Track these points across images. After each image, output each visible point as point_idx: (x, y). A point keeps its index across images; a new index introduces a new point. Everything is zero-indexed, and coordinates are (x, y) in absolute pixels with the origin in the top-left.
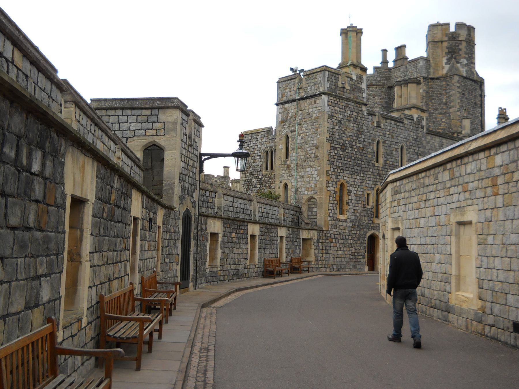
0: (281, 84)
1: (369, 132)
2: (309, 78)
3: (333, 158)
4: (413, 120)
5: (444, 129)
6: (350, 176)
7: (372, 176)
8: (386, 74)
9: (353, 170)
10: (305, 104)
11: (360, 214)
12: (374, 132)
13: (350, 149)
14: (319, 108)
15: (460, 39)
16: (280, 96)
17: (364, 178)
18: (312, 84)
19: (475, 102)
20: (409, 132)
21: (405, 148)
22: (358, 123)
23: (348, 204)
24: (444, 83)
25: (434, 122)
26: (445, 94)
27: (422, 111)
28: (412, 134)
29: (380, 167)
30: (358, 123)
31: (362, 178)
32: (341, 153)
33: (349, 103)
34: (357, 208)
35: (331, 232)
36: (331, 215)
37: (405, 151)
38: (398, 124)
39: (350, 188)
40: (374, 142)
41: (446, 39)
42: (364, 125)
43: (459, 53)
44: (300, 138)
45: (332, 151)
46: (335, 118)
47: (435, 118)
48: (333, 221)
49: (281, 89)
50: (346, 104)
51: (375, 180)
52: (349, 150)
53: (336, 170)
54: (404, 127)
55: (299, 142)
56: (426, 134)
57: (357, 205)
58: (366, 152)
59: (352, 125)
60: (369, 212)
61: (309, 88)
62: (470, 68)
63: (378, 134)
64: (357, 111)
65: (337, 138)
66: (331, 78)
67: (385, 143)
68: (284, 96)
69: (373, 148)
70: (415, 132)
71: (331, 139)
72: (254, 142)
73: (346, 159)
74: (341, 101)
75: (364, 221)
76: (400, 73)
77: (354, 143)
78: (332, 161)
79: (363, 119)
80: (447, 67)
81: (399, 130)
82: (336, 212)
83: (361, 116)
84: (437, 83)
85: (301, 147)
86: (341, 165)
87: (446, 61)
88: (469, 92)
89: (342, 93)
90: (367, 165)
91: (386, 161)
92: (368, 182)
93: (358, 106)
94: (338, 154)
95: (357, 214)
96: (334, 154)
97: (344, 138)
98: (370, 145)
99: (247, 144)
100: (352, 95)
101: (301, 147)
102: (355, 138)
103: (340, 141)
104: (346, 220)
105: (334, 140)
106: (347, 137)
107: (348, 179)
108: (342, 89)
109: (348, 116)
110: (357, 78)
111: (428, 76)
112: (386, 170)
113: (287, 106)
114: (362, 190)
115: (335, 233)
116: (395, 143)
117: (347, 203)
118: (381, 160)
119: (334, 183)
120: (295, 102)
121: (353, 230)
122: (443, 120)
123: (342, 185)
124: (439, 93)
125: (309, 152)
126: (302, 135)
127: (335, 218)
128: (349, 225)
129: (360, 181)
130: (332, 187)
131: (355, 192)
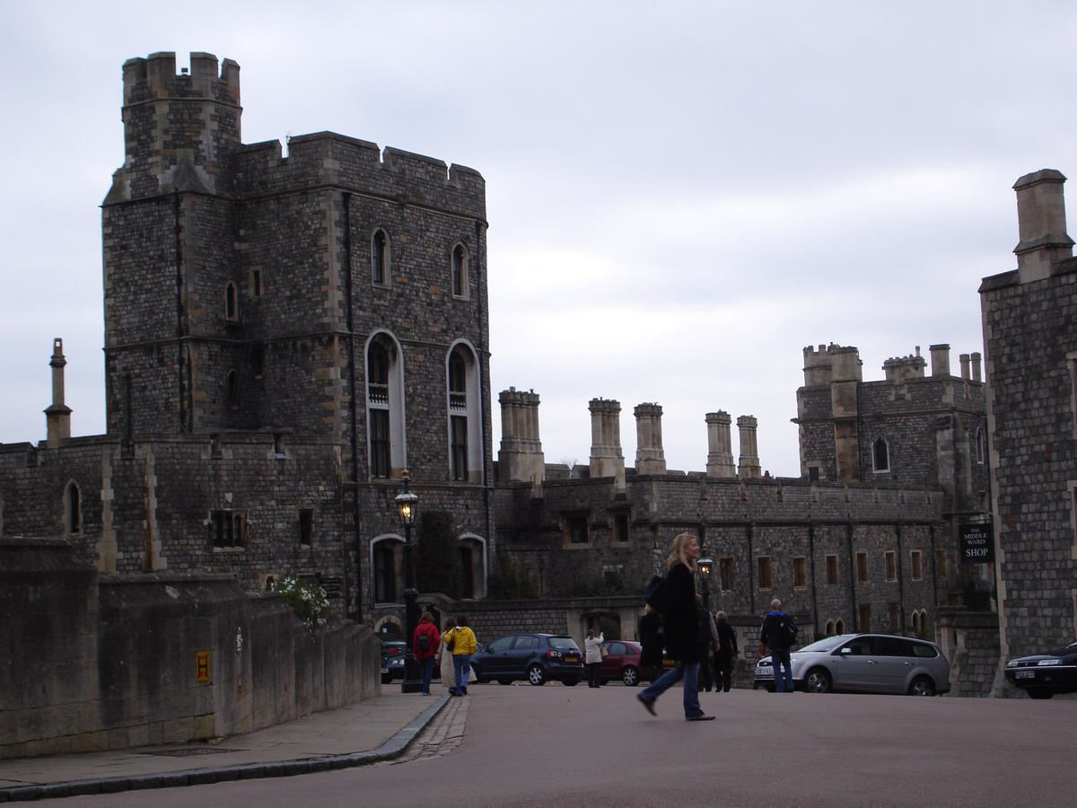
62: (145, 170)
88: (141, 236)
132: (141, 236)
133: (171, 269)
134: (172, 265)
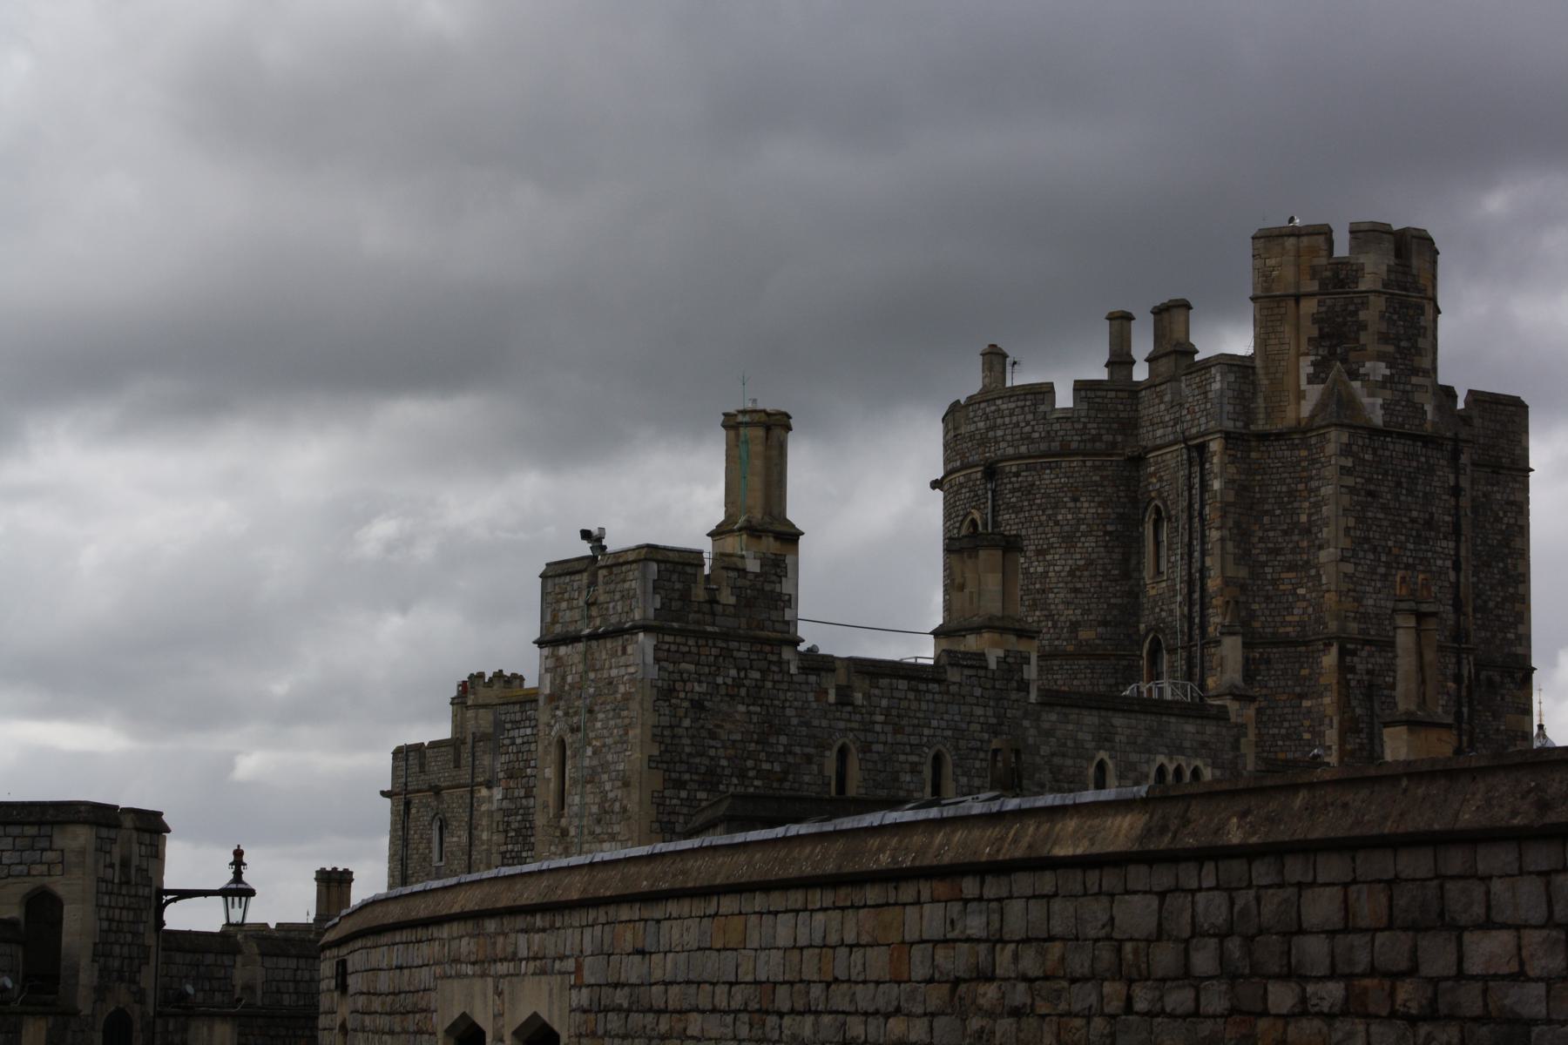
0: (550, 583)
1: (807, 724)
2: (613, 577)
4: (986, 668)
5: (1301, 624)
8: (1121, 407)
10: (603, 650)
12: (825, 723)
13: (735, 781)
14: (632, 670)
15: (1362, 287)
16: (548, 619)
18: (618, 596)
19: (1427, 516)
20: (965, 709)
21: (949, 759)
22: (767, 702)
24: (1304, 453)
25: (1268, 598)
26: (1305, 494)
28: (979, 711)
30: (767, 702)
32: (701, 795)
33: (733, 645)
37: (948, 770)
38: (922, 687)
40: (827, 753)
41: (1314, 286)
42: (788, 704)
43: (1357, 340)
44: (589, 751)
46: (682, 695)
47: (1274, 582)
49: (550, 599)
50: (722, 649)
54: (947, 692)
55: (587, 762)
59: (742, 708)
61: (611, 605)
62: (1404, 392)
63: (842, 725)
64: (764, 665)
65: (689, 755)
66: (669, 580)
67: (870, 751)
68: (558, 622)
69: (821, 772)
70: (991, 703)
71: (667, 757)
72: (529, 731)
74: (701, 642)
76: (1162, 407)
78: (669, 822)
79: (785, 686)
80: (1314, 393)
81: (924, 706)
83: (777, 677)
84: (1279, 454)
85: (591, 778)
87: (1311, 370)
88: (1399, 484)
89: (708, 618)
93: (767, 648)
96: (675, 801)
97: (712, 752)
99: (512, 734)
100: (743, 621)
101: (591, 778)
102: (752, 747)
103: (697, 760)
105: (677, 759)
106: (724, 747)
108: (706, 608)
109: (729, 681)
110: (762, 566)
111: (1246, 425)
113: (563, 650)
116: (908, 749)
120: (581, 644)
122: (1301, 591)
124: (1284, 489)
125: (611, 795)
126: (594, 743)
132: (1399, 484)
133: (1444, 544)
134: (1445, 538)
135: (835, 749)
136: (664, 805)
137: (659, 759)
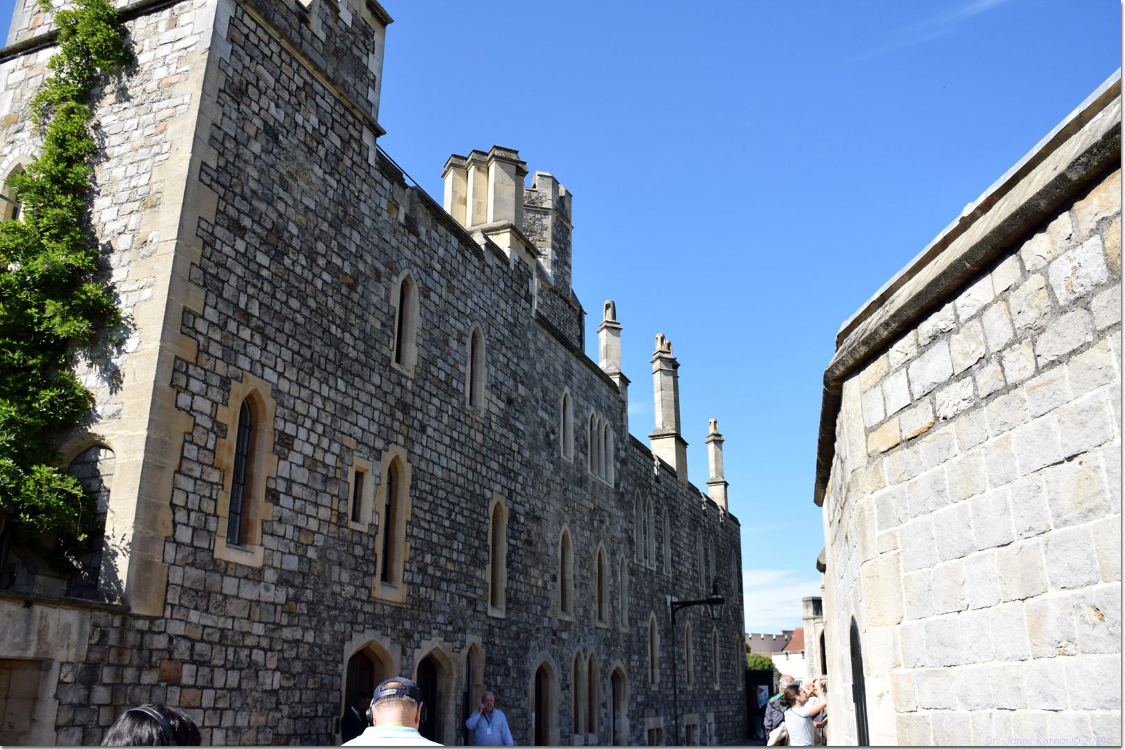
3: (224, 266)
6: (291, 374)
7: (378, 404)
9: (307, 353)
11: (322, 551)
17: (348, 402)
21: (483, 342)
22: (344, 181)
23: (272, 495)
27: (528, 250)
29: (407, 378)
30: (344, 181)
31: (339, 398)
32: (263, 259)
34: (313, 524)
35: (177, 628)
36: (184, 535)
39: (290, 429)
40: (394, 279)
45: (220, 232)
48: (194, 573)
50: (305, 83)
51: (388, 420)
52: (296, 262)
53: (232, 326)
54: (483, 272)
56: (536, 324)
57: (310, 510)
58: (364, 303)
59: (320, 172)
60: (358, 551)
63: (408, 253)
65: (254, 192)
69: (387, 298)
73: (281, 296)
75: (337, 589)
77: (321, 247)
82: (212, 525)
83: (357, 159)
86: (255, 309)
90: (365, 353)
91: (427, 363)
92: (363, 422)
93: (351, 119)
94: (245, 258)
95: (311, 553)
96: (227, 250)
97: (281, 207)
98: (378, 280)
102: (325, 226)
104: (260, 571)
106: (295, 207)
107: (284, 386)
109: (310, 130)
112: (425, 395)
114: (336, 448)
115: (196, 634)
117: (268, 490)
118: (412, 354)
119: (215, 381)
121: (289, 625)
123: (249, 410)
127: (203, 556)
128: (268, 596)
129: (330, 407)
130: (205, 396)
131: (308, 450)
135: (402, 278)
136: (213, 248)
137: (215, 175)
